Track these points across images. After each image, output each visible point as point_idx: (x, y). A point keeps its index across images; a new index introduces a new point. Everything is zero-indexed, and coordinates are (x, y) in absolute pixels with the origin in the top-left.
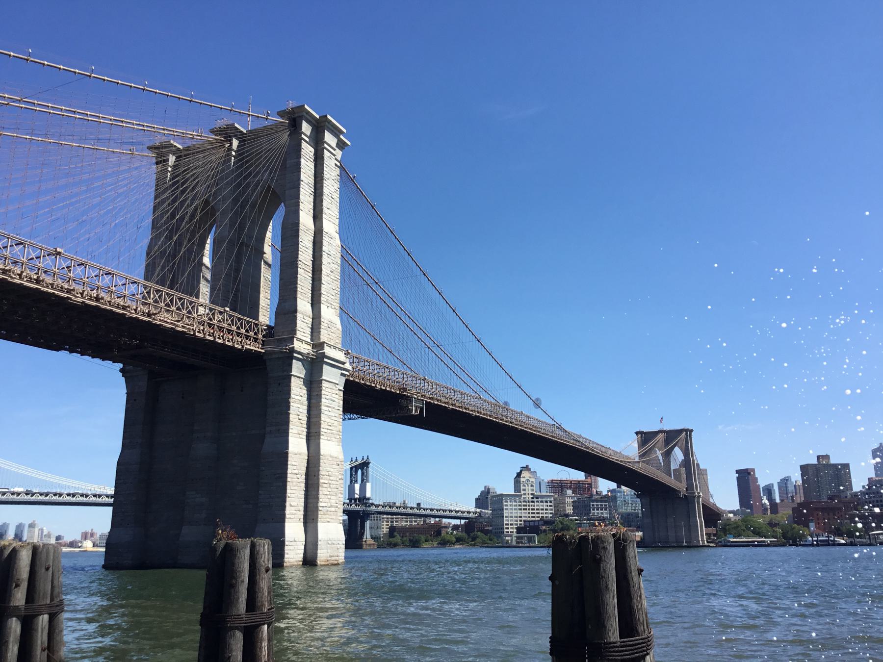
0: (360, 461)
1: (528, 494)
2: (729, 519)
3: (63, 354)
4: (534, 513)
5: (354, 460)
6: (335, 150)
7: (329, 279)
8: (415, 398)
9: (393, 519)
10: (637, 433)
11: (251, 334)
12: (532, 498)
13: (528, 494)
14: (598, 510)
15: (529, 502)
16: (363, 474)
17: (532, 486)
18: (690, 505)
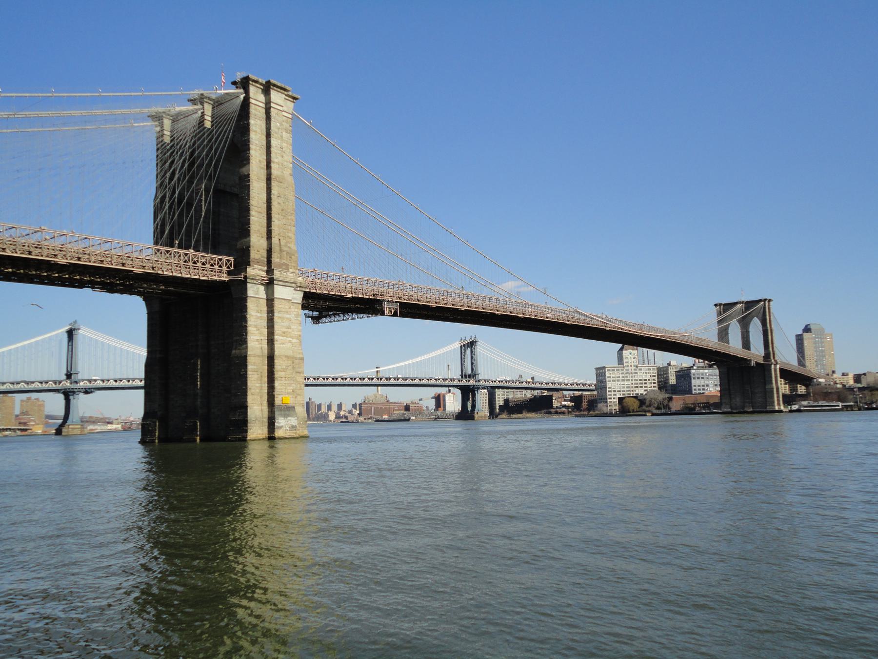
0: (468, 340)
1: (631, 366)
2: (819, 384)
3: (87, 291)
4: (637, 384)
5: (463, 339)
6: (282, 106)
7: (280, 216)
8: (388, 301)
9: (508, 392)
10: (716, 305)
11: (216, 267)
12: (635, 370)
13: (631, 366)
14: (698, 378)
15: (631, 373)
16: (472, 352)
17: (634, 358)
18: (766, 373)
